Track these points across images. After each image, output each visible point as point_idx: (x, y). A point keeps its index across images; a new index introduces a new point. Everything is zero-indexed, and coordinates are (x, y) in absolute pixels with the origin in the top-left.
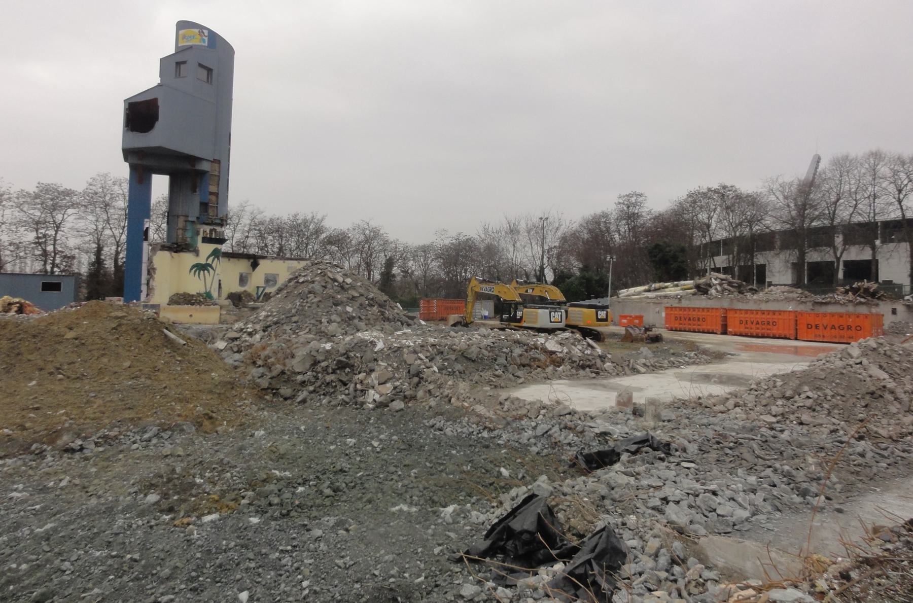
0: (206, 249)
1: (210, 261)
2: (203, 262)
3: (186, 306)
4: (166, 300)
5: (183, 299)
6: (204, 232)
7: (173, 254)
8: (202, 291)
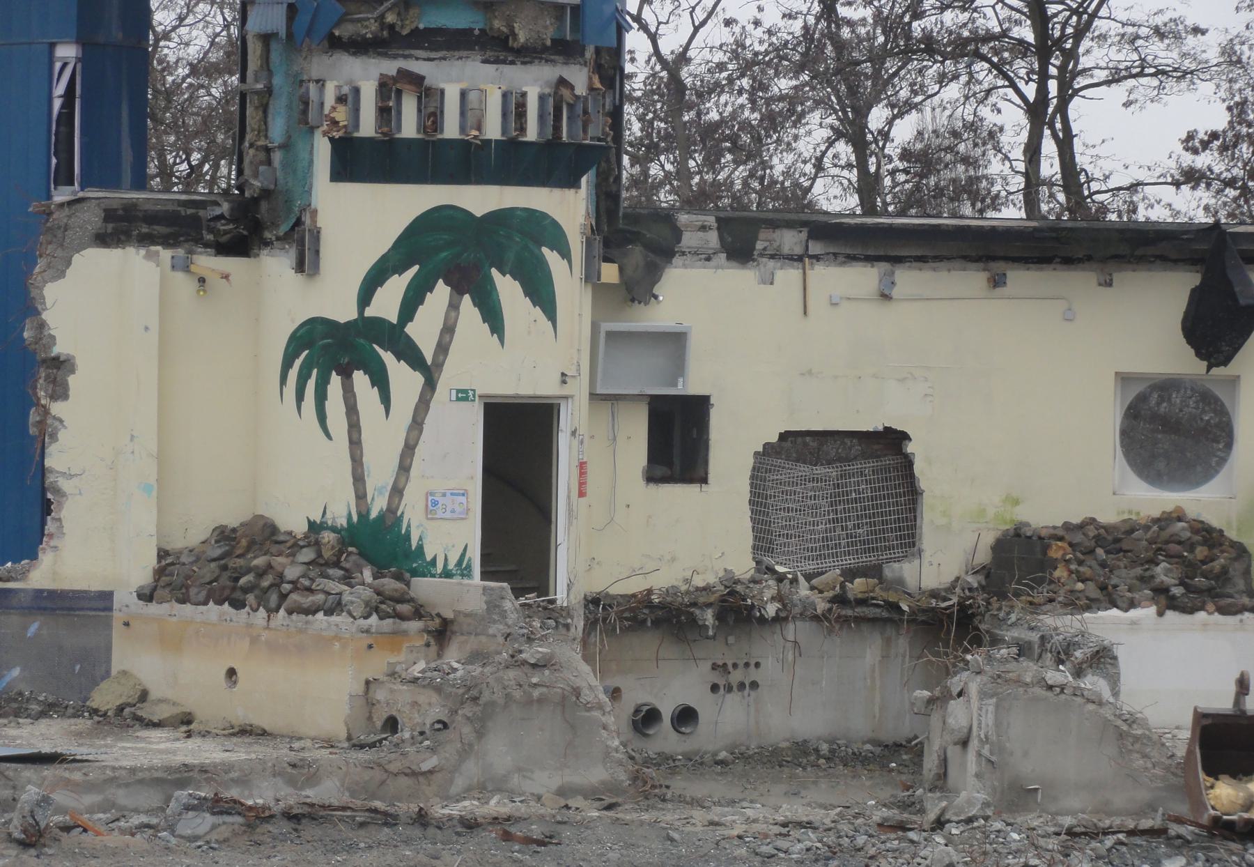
0: (361, 221)
1: (387, 303)
2: (345, 312)
3: (213, 611)
4: (141, 570)
5: (236, 569)
6: (349, 99)
7: (207, 262)
8: (341, 509)
